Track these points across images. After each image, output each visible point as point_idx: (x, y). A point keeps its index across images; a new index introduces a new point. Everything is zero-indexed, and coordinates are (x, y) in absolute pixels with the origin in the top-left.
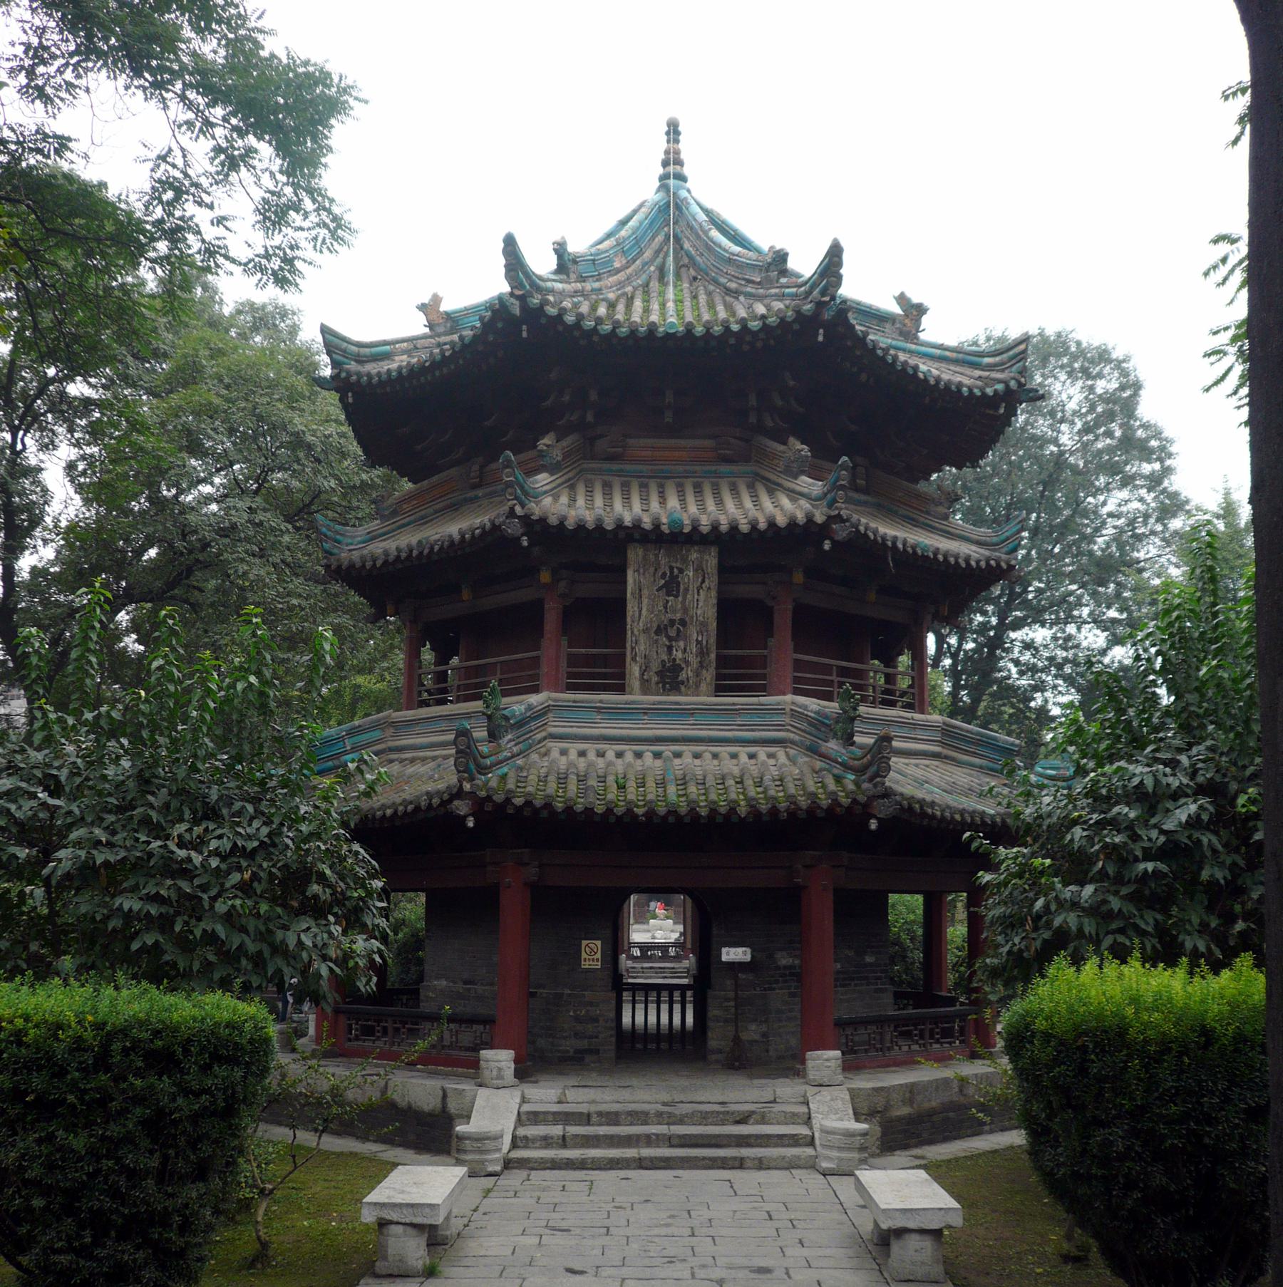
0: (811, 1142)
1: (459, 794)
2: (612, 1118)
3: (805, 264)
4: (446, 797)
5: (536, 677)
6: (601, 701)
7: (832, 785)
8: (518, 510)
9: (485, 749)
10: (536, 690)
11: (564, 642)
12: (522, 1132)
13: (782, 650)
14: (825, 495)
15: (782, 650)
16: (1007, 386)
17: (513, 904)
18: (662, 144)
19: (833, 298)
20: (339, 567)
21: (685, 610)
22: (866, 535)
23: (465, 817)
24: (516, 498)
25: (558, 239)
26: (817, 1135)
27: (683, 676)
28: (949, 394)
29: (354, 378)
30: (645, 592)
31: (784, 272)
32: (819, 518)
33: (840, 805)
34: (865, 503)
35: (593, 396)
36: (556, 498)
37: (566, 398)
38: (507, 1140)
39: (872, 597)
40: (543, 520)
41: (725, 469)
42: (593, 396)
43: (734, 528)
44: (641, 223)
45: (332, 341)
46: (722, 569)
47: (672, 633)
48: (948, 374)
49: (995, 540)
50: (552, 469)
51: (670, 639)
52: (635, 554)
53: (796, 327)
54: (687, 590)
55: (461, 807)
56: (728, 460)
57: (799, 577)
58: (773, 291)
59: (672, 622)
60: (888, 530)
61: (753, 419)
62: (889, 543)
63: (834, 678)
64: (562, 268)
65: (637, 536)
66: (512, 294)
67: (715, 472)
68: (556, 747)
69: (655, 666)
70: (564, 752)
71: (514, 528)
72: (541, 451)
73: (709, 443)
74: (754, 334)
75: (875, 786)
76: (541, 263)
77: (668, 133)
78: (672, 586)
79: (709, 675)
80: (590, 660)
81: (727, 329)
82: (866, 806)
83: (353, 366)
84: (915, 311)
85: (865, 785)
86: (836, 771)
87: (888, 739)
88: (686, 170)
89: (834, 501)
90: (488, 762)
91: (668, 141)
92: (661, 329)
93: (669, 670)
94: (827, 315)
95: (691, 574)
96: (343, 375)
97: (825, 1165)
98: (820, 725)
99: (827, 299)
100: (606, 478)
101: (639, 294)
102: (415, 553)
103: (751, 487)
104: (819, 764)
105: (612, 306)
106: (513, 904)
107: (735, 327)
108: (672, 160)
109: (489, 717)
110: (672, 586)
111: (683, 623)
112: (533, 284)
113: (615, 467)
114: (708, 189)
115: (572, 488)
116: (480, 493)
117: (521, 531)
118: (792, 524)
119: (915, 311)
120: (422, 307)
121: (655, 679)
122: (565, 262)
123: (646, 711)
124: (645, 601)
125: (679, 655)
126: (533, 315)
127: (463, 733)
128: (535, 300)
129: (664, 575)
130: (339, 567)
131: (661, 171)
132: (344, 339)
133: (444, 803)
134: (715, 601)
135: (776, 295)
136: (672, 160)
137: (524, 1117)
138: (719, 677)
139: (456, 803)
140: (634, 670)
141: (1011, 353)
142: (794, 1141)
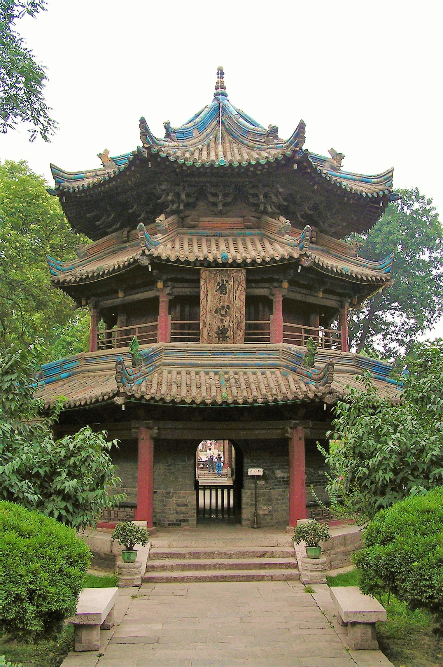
0: (296, 566)
1: (118, 394)
2: (196, 555)
3: (285, 134)
4: (111, 395)
5: (156, 335)
6: (188, 347)
7: (304, 388)
8: (147, 253)
9: (130, 371)
10: (155, 341)
11: (170, 316)
12: (151, 563)
13: (277, 320)
14: (299, 244)
15: (277, 320)
16: (384, 193)
17: (145, 449)
18: (215, 79)
19: (301, 148)
20: (59, 281)
21: (230, 302)
22: (318, 264)
23: (121, 405)
24: (145, 246)
25: (166, 121)
26: (300, 563)
27: (228, 334)
28: (358, 196)
29: (67, 189)
30: (209, 293)
31: (276, 137)
32: (296, 256)
33: (308, 397)
34: (316, 249)
35: (183, 196)
36: (165, 246)
37: (170, 198)
38: (144, 568)
39: (321, 294)
40: (159, 257)
41: (247, 232)
42: (183, 196)
43: (254, 262)
44: (205, 116)
45: (56, 172)
46: (248, 281)
47: (223, 312)
48: (357, 187)
49: (379, 267)
50: (164, 232)
51: (222, 316)
52: (205, 274)
53: (283, 162)
54: (230, 291)
55: (119, 400)
56: (249, 228)
57: (285, 285)
58: (271, 146)
59: (223, 307)
60: (328, 262)
61: (262, 207)
62: (330, 268)
63: (303, 334)
64: (168, 135)
65: (206, 264)
66: (143, 147)
67: (243, 234)
68: (165, 370)
69: (215, 329)
70: (170, 372)
71: (145, 262)
72: (158, 223)
73: (239, 219)
74: (263, 166)
75: (326, 388)
76: (158, 133)
77: (218, 74)
78: (222, 289)
79: (241, 333)
80: (182, 327)
81: (249, 163)
82: (321, 399)
83: (66, 184)
84: (339, 157)
85: (321, 388)
86: (305, 381)
87: (332, 364)
88: (227, 91)
89: (303, 247)
90: (132, 377)
91: (218, 78)
92: (217, 163)
93: (221, 331)
94: (298, 157)
95: (232, 283)
96: (61, 188)
97: (304, 579)
98: (297, 357)
99: (298, 149)
100: (190, 237)
101: (205, 148)
102: (95, 274)
103: (261, 240)
104: (297, 377)
105: (192, 154)
106: (145, 449)
107: (253, 163)
108: (220, 87)
109: (133, 355)
110: (222, 289)
111: (228, 307)
112: (154, 142)
113: (193, 231)
114: (237, 101)
115: (173, 241)
116: (127, 245)
117: (148, 262)
118: (283, 259)
119: (339, 157)
120: (100, 156)
121: (215, 335)
122: (169, 132)
123: (210, 351)
124: (210, 297)
125: (227, 323)
126: (154, 157)
127: (120, 363)
128: (155, 150)
129: (219, 283)
130: (59, 281)
131: (215, 91)
132: (61, 171)
133: (110, 398)
134: (243, 296)
135: (272, 148)
136: (220, 87)
137: (152, 556)
138: (246, 334)
139: (116, 398)
140: (204, 332)
141: (385, 177)
142: (288, 566)
